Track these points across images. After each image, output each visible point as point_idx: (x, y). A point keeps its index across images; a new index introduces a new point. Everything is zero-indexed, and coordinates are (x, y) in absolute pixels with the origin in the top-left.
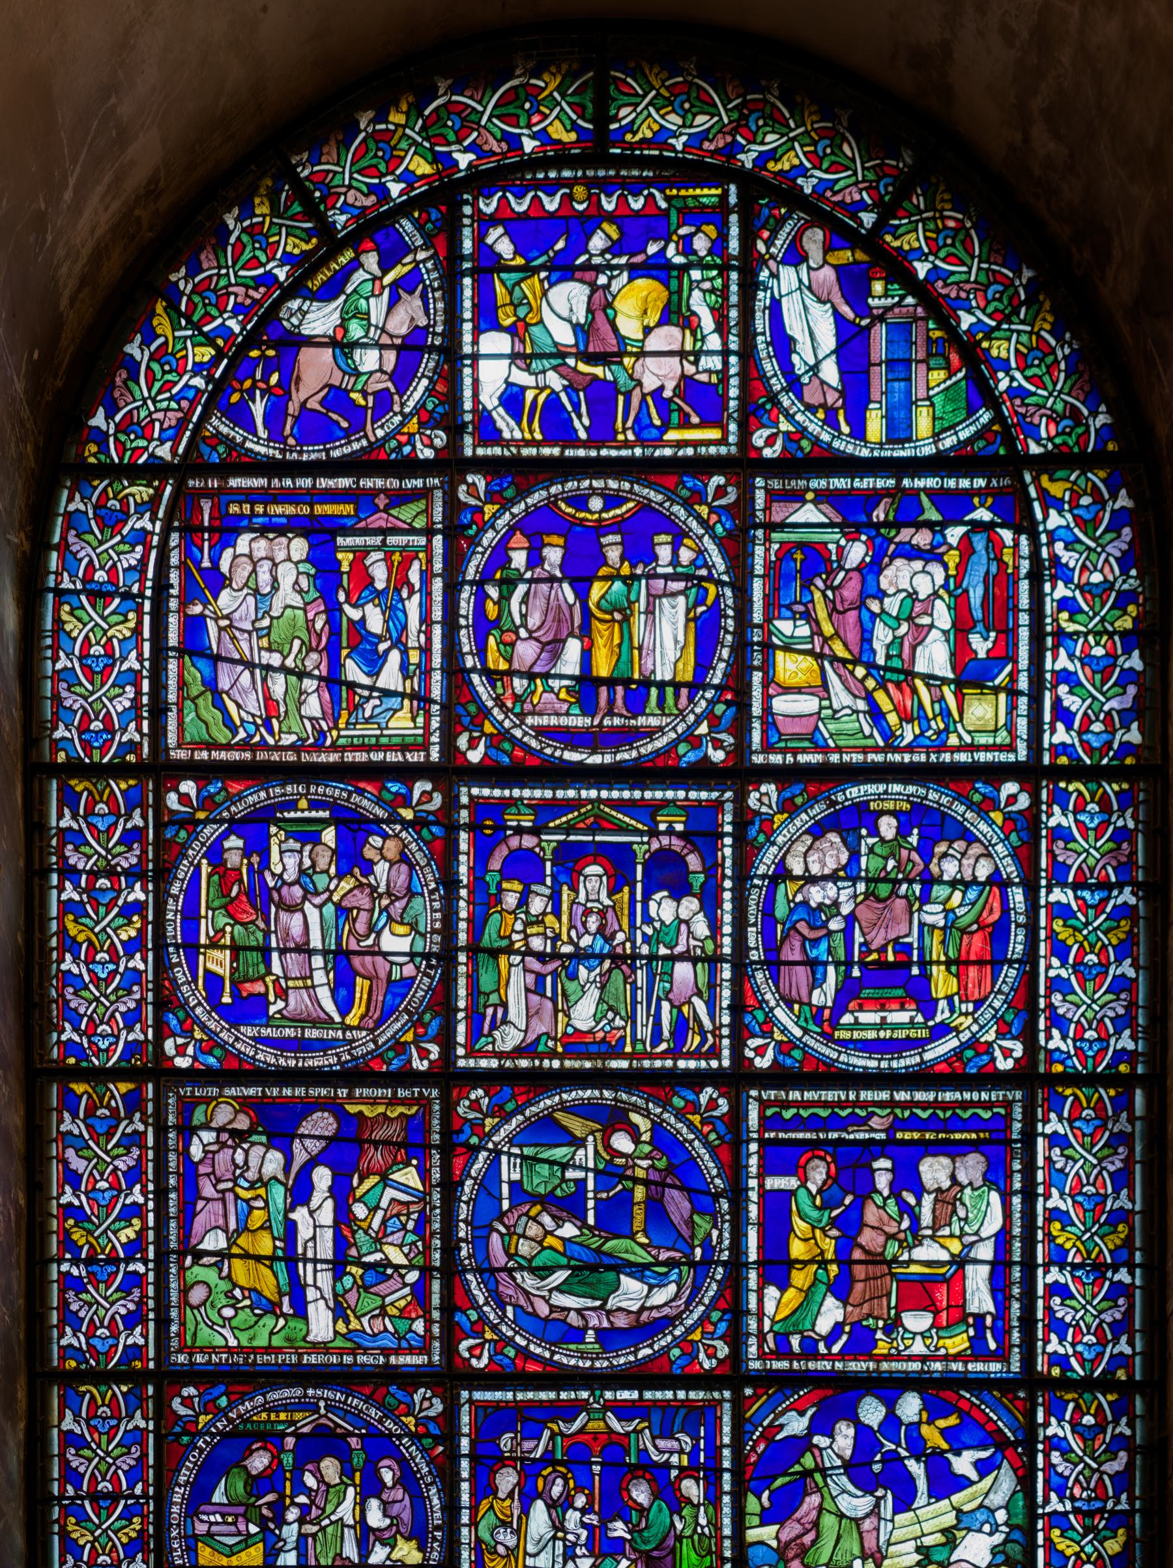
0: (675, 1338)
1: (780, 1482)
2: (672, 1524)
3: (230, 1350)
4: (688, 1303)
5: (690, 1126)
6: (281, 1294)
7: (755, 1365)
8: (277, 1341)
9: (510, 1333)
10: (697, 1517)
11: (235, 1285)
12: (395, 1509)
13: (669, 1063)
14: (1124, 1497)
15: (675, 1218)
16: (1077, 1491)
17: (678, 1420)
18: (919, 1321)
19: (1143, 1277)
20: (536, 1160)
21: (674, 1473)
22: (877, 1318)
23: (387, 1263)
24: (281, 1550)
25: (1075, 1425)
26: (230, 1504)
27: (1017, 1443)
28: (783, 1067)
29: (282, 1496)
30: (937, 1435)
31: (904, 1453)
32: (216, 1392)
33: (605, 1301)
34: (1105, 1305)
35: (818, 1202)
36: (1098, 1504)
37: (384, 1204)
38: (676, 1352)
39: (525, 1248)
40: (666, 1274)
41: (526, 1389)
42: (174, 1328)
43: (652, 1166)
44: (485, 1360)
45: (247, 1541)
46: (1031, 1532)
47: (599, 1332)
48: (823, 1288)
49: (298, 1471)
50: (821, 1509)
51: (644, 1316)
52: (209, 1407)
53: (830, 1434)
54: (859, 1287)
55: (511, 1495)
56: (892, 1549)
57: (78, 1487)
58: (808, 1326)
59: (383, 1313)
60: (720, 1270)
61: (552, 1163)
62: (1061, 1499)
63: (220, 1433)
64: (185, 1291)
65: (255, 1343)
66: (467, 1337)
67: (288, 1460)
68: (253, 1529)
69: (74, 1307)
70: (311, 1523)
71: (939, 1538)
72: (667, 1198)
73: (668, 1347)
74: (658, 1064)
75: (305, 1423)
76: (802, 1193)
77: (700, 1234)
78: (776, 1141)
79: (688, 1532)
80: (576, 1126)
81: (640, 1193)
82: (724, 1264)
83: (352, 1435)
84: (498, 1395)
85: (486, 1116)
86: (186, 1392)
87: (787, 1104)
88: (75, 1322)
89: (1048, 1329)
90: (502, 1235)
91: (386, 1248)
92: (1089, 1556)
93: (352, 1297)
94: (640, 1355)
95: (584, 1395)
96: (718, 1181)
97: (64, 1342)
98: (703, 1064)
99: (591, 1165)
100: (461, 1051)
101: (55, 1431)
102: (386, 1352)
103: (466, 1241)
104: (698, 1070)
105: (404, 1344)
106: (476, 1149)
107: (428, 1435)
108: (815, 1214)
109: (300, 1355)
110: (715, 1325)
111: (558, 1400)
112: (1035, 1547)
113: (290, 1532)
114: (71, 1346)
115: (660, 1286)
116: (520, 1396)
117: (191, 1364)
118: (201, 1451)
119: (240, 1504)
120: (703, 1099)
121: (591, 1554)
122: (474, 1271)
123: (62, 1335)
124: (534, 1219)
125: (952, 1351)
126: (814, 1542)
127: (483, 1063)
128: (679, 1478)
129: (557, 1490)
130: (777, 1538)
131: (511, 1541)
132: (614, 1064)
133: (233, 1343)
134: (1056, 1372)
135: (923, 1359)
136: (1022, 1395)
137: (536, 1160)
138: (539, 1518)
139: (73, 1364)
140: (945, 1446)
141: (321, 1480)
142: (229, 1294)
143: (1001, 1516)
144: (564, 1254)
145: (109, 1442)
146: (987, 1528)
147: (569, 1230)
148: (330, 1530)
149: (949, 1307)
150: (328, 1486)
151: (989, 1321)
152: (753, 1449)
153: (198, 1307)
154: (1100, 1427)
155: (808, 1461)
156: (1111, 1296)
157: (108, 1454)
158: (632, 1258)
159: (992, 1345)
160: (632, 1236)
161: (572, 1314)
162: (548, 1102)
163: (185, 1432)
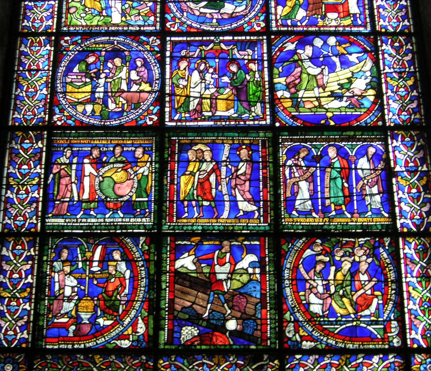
1: (285, 64)
2: (246, 77)
3: (83, 26)
4: (249, 11)
6: (102, 9)
7: (275, 29)
8: (100, 23)
9: (185, 20)
10: (254, 75)
11: (86, 7)
12: (141, 74)
14: (412, 67)
16: (395, 66)
17: (247, 46)
18: (332, 16)
19: (410, 3)
21: (246, 61)
22: (318, 15)
24: (98, 87)
25: (392, 46)
26: (80, 72)
27: (371, 52)
29: (99, 70)
30: (343, 49)
31: (330, 54)
32: (77, 38)
33: (220, 11)
34: (398, 11)
36: (403, 70)
38: (246, 25)
40: (241, 3)
41: (191, 36)
42: (63, 20)
44: (176, 28)
45: (85, 84)
46: (379, 79)
47: (217, 19)
48: (298, 6)
49: (106, 61)
50: (301, 72)
51: (234, 15)
52: (75, 43)
53: (304, 50)
54: (311, 6)
55: (185, 69)
56: (328, 85)
57: (24, 68)
59: (139, 14)
62: (390, 68)
63: (77, 50)
64: (68, 9)
65: (92, 24)
66: (170, 21)
67: (102, 59)
68: (88, 80)
69: (28, 14)
70: (110, 78)
71: (346, 81)
73: (243, 24)
75: (109, 47)
79: (252, 80)
83: (126, 51)
86: (66, 38)
88: (28, 19)
89: (379, 18)
92: (401, 86)
93: (128, 11)
94: (233, 26)
95: (212, 38)
97: (24, 24)
101: (18, 51)
102: (140, 26)
107: (154, 51)
109: (108, 28)
110: (260, 17)
111: (202, 40)
112: (381, 83)
113: (102, 81)
114: (26, 25)
116: (188, 39)
117: (69, 30)
118: (70, 56)
119: (84, 72)
121: (215, 87)
123: (23, 22)
125: (346, 24)
126: (299, 83)
128: (248, 63)
129: (202, 67)
130: (285, 81)
131: (185, 83)
133: (84, 24)
134: (383, 30)
135: (336, 27)
136: (372, 37)
138: (196, 76)
139: (26, 31)
140: (346, 52)
141: (114, 65)
142: (83, 10)
143: (368, 74)
145: (37, 54)
146: (363, 77)
148: (117, 80)
149: (343, 12)
150: (117, 67)
151: (358, 16)
152: (275, 54)
153: (72, 14)
154: (401, 46)
155: (296, 57)
156: (401, 8)
157: (36, 57)
159: (360, 22)
163: (65, 50)
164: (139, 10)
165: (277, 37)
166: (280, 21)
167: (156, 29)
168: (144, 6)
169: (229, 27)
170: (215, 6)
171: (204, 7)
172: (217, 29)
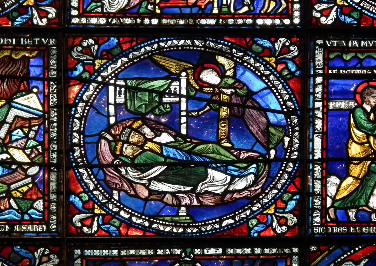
0: (253, 212)
4: (263, 189)
5: (266, 65)
7: (321, 230)
9: (115, 209)
13: (249, 21)
15: (254, 129)
20: (137, 89)
23: (13, 161)
28: (344, 23)
33: (195, 187)
35: (372, 117)
37: (10, 119)
39: (128, 151)
40: (246, 169)
43: (235, 93)
44: (95, 228)
58: (362, 202)
60: (291, 165)
61: (151, 91)
66: (80, 212)
72: (247, 115)
73: (248, 219)
74: (240, 21)
76: (359, 113)
77: (275, 140)
78: (338, 76)
80: (172, 66)
81: (224, 112)
82: (294, 161)
84: (105, 252)
85: (96, 58)
87: (347, 50)
90: (109, 142)
91: (11, 150)
94: (224, 224)
95: (178, 251)
96: (289, 103)
98: (278, 22)
99: (184, 92)
100: (74, 12)
103: (79, 145)
104: (273, 25)
105: (26, 217)
106: (88, 81)
108: (369, 126)
110: (286, 203)
115: (241, 177)
120: (278, 46)
122: (85, 167)
124: (137, 130)
127: (94, 21)
132: (204, 22)
137: (137, 89)
144: (161, 155)
147: (165, 138)
158: (218, 157)
160: (218, 142)
161: (168, 195)
162: (148, 48)
164: (9, 185)
165: (322, 248)
166: (331, 211)
167: (49, 230)
168: (19, 175)
169: (217, 226)
170: (183, 176)
171: (157, 179)
172: (189, 231)
